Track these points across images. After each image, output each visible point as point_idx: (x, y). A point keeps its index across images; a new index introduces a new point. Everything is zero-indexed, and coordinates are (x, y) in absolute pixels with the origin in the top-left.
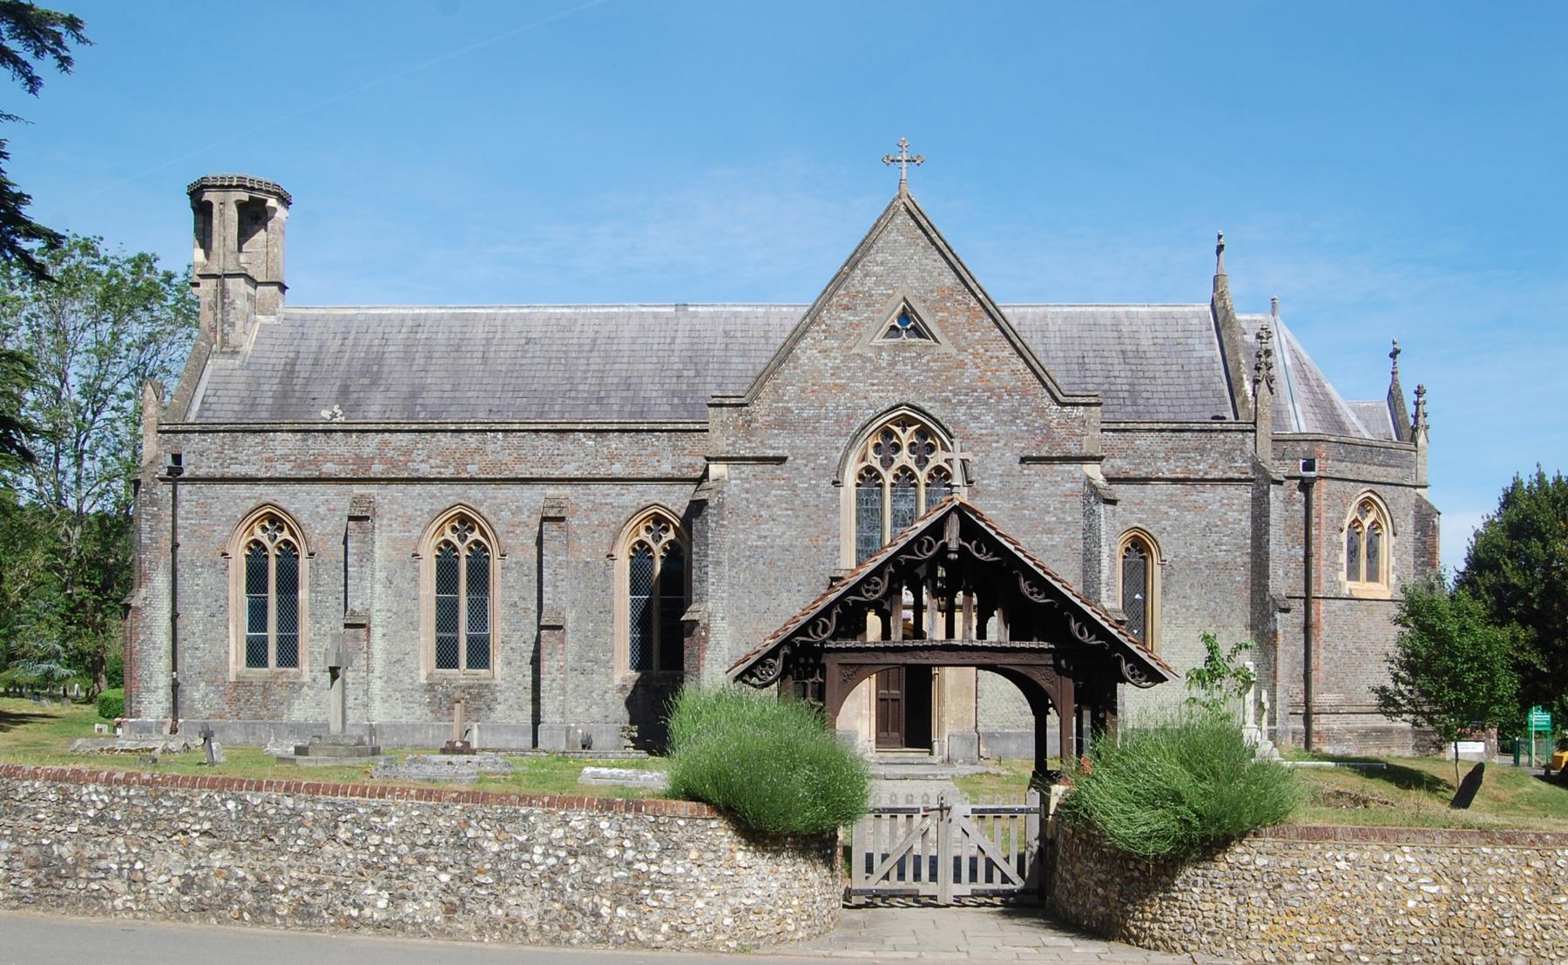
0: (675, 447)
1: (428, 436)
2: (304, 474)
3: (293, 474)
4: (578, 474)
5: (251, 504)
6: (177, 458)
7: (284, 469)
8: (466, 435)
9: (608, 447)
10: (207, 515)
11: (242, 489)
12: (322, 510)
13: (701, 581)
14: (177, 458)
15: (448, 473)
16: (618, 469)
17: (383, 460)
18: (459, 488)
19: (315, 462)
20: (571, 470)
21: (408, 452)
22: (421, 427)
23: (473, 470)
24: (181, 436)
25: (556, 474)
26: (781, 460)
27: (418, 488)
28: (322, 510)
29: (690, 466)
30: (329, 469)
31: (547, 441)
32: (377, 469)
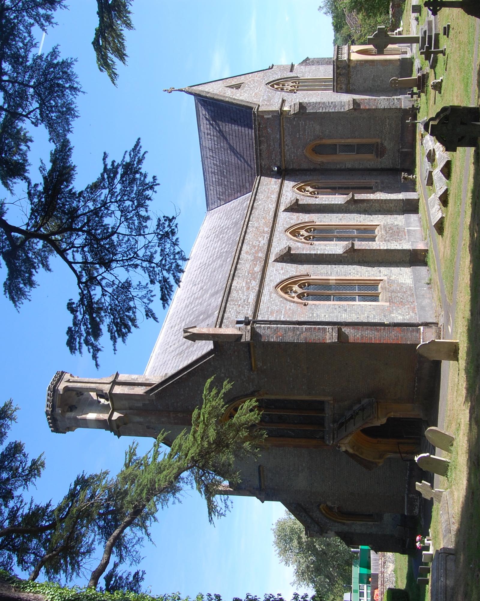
0: (265, 185)
1: (246, 241)
2: (259, 277)
3: (258, 281)
4: (274, 205)
5: (274, 295)
6: (238, 322)
7: (255, 284)
8: (248, 231)
9: (262, 199)
10: (279, 312)
11: (264, 298)
12: (281, 272)
13: (335, 106)
14: (238, 322)
15: (267, 236)
16: (274, 197)
17: (257, 252)
18: (276, 234)
19: (253, 274)
20: (273, 207)
21: (254, 247)
22: (241, 242)
23: (268, 229)
24: (224, 321)
25: (273, 209)
26: (283, 101)
27: (274, 244)
28: (281, 272)
29: (276, 182)
30: (258, 269)
31: (255, 213)
32: (262, 255)
